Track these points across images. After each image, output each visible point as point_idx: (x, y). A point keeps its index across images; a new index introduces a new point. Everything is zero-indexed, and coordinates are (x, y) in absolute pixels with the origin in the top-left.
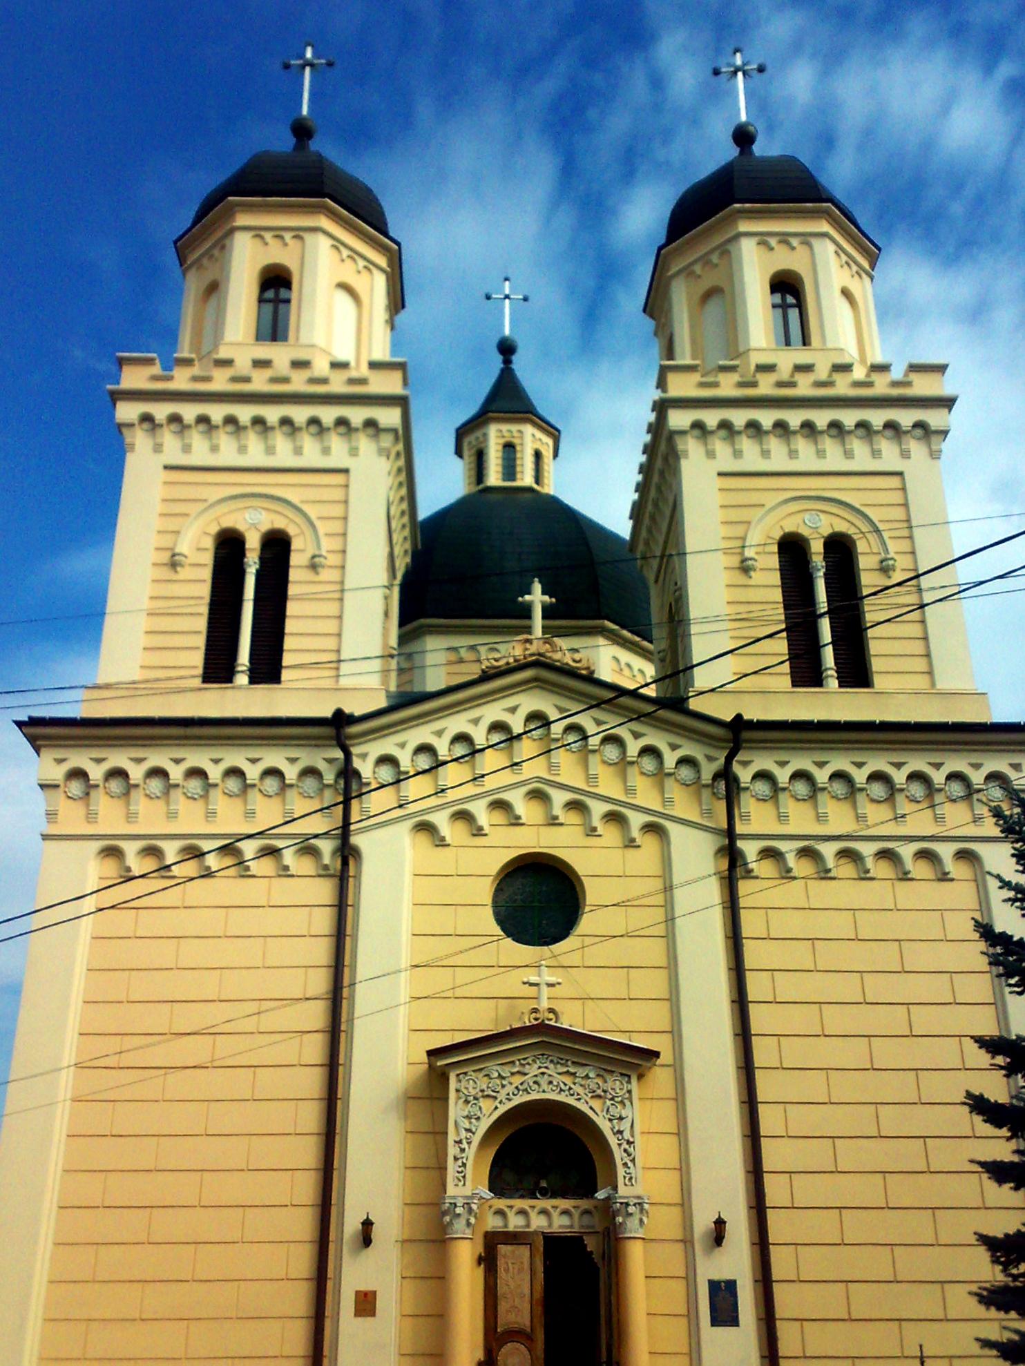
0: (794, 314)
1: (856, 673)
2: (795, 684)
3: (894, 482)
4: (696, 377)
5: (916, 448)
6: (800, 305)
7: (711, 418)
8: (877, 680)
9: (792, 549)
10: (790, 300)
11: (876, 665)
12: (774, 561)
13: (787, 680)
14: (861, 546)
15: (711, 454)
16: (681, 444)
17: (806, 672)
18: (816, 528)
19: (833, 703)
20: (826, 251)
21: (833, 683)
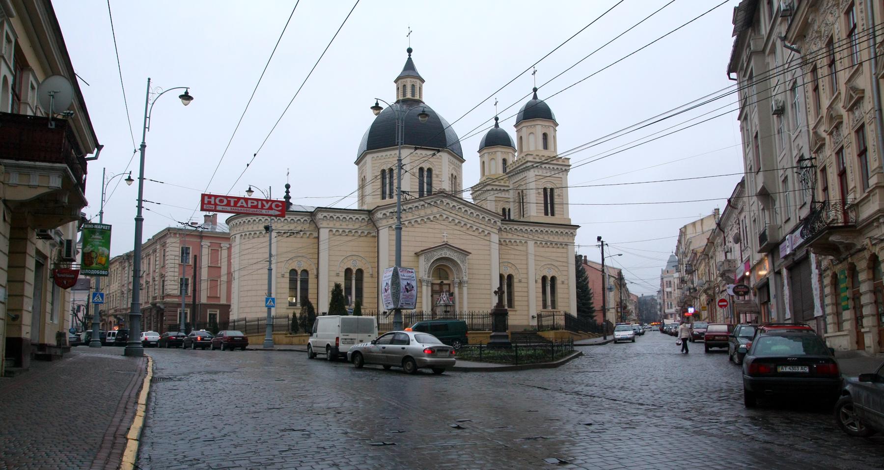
1: (553, 214)
9: (545, 189)
17: (546, 214)
19: (549, 219)
20: (551, 129)
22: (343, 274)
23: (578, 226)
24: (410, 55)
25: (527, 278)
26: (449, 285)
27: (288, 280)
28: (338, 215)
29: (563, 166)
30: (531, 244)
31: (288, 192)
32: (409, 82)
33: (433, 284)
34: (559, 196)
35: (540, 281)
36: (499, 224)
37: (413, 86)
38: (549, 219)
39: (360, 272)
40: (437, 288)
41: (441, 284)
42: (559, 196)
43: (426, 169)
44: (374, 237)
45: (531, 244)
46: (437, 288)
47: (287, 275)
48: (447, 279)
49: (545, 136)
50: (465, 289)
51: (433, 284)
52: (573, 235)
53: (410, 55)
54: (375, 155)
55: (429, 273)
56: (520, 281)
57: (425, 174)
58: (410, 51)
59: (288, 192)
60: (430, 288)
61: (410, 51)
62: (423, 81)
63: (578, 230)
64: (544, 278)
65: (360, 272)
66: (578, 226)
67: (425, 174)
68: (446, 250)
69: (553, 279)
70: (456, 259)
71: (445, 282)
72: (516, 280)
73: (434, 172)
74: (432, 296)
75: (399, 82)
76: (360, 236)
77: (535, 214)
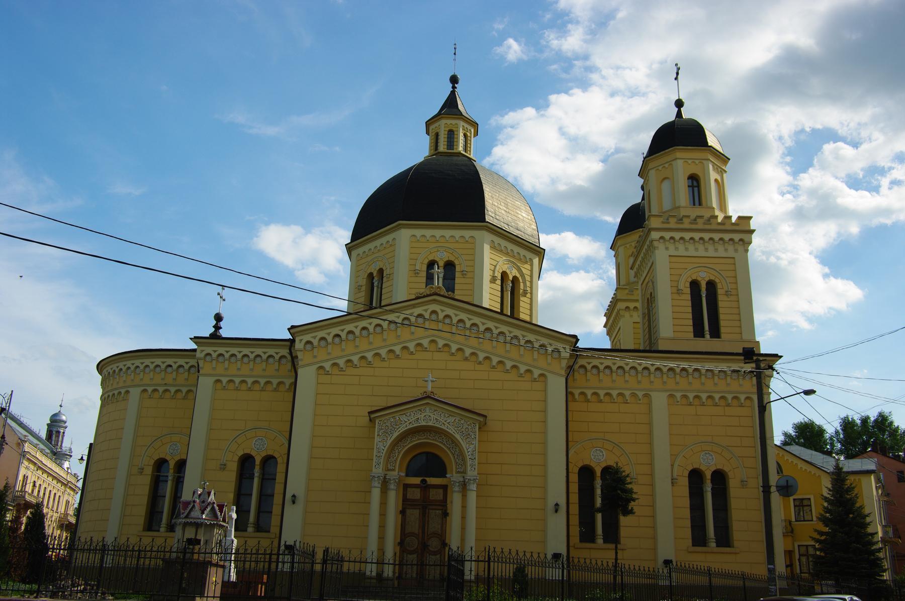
0: (696, 189)
1: (716, 333)
2: (695, 336)
3: (731, 261)
4: (661, 219)
5: (741, 248)
6: (698, 186)
7: (667, 235)
8: (723, 335)
9: (695, 285)
10: (695, 184)
11: (722, 330)
12: (688, 291)
13: (692, 335)
14: (719, 286)
15: (667, 248)
16: (655, 244)
17: (698, 332)
18: (703, 278)
21: (708, 336)
22: (233, 467)
23: (777, 357)
24: (454, 87)
25: (652, 475)
26: (445, 488)
28: (234, 350)
30: (660, 400)
31: (217, 327)
33: (406, 486)
34: (727, 293)
35: (685, 481)
37: (451, 135)
38: (707, 343)
40: (415, 494)
42: (727, 293)
45: (660, 400)
49: (695, 182)
50: (472, 496)
53: (454, 87)
58: (454, 80)
59: (217, 327)
61: (454, 80)
64: (695, 476)
68: (428, 412)
70: (451, 430)
71: (432, 481)
73: (458, 268)
74: (403, 512)
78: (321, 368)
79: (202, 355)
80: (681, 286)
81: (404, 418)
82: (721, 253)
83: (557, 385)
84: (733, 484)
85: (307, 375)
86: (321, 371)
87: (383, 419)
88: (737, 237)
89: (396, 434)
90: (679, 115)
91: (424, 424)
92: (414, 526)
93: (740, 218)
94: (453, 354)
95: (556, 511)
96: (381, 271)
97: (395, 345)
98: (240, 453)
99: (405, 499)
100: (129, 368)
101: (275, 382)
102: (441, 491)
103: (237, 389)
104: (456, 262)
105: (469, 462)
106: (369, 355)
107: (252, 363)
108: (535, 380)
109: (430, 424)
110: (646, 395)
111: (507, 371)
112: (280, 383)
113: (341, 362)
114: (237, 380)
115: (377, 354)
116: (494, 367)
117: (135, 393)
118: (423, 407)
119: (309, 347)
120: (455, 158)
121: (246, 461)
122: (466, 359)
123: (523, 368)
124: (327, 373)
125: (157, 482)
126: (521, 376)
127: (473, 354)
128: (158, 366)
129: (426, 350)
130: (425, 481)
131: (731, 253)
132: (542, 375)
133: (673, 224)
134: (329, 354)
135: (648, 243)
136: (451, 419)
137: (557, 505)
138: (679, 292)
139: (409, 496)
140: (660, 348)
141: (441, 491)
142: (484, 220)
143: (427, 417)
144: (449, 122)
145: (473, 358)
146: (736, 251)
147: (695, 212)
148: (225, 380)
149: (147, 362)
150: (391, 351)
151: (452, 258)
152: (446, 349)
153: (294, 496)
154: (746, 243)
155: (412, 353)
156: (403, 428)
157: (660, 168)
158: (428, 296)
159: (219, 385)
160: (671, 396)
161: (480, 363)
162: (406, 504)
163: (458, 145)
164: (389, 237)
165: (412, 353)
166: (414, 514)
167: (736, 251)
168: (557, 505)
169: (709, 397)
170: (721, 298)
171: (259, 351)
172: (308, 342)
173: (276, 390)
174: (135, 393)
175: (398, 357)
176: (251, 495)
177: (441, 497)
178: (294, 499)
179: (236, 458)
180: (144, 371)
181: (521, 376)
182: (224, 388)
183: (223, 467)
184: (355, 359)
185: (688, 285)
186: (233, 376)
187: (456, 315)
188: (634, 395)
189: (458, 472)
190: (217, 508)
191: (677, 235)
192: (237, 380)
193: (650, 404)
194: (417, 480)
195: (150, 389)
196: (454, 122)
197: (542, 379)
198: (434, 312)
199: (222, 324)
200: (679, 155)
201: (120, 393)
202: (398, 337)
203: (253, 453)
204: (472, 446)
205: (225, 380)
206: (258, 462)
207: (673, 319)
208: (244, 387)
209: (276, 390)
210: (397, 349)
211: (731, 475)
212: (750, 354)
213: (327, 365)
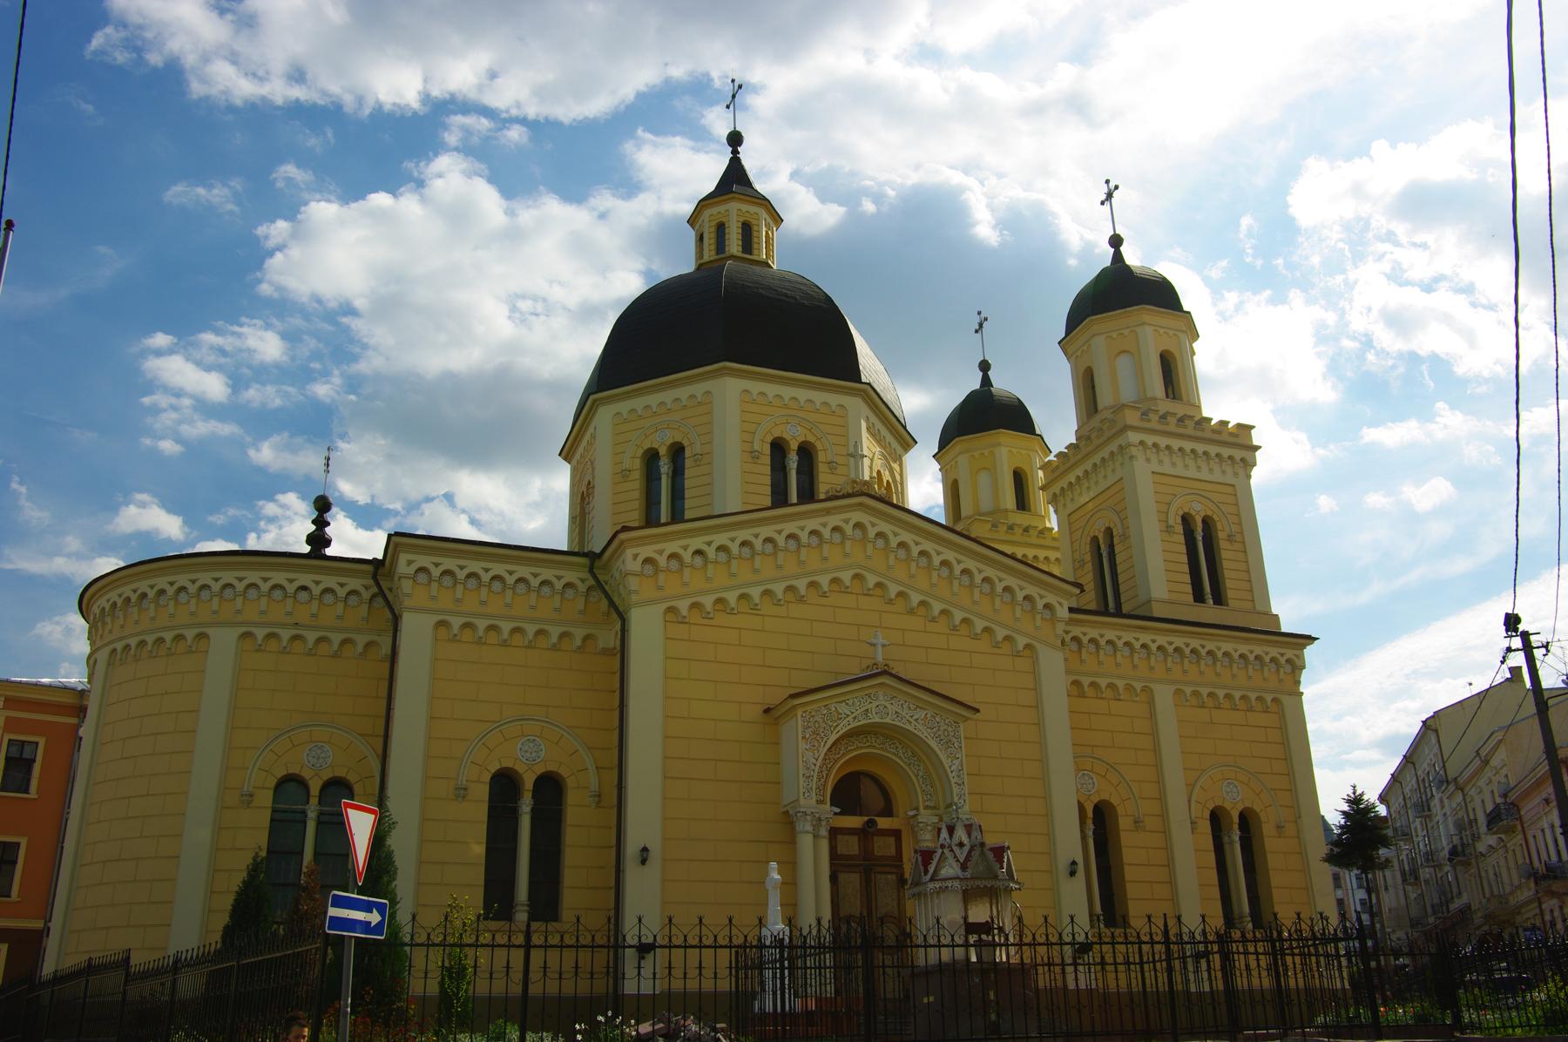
1: (1219, 599)
3: (1230, 490)
5: (1241, 472)
7: (1150, 439)
9: (1186, 520)
11: (1230, 594)
12: (1180, 529)
15: (1148, 460)
17: (1199, 597)
18: (1198, 510)
22: (482, 792)
23: (1311, 639)
24: (735, 152)
26: (896, 834)
27: (265, 819)
29: (1237, 445)
30: (1164, 696)
32: (734, 211)
34: (1230, 538)
35: (1205, 827)
36: (1063, 613)
38: (1208, 612)
39: (550, 787)
40: (850, 846)
41: (867, 833)
42: (1230, 538)
43: (794, 446)
44: (606, 652)
46: (850, 846)
47: (266, 799)
48: (888, 812)
51: (834, 832)
52: (1296, 667)
53: (735, 152)
54: (624, 407)
55: (821, 789)
56: (1137, 823)
57: (793, 462)
60: (824, 845)
62: (778, 220)
63: (1309, 652)
64: (1217, 819)
65: (550, 787)
66: (1311, 639)
67: (793, 462)
69: (1247, 821)
70: (923, 733)
71: (883, 823)
72: (1124, 823)
73: (821, 457)
74: (834, 878)
75: (707, 213)
76: (555, 648)
77: (1166, 596)
78: (671, 610)
79: (412, 569)
80: (1171, 522)
81: (843, 709)
82: (1217, 476)
83: (1053, 664)
84: (1268, 830)
85: (416, 629)
86: (670, 617)
87: (809, 708)
88: (1238, 454)
89: (833, 738)
90: (1118, 257)
91: (877, 719)
92: (853, 906)
93: (1239, 426)
94: (890, 602)
95: (1072, 873)
96: (677, 451)
97: (797, 577)
98: (494, 768)
99: (834, 855)
100: (162, 592)
101: (555, 631)
102: (891, 840)
103: (480, 642)
104: (819, 447)
105: (955, 790)
106: (755, 592)
107: (315, 603)
108: (1017, 655)
109: (888, 720)
110: (1144, 689)
111: (976, 637)
112: (564, 635)
113: (708, 601)
114: (482, 624)
115: (767, 593)
116: (954, 628)
117: (224, 641)
118: (872, 691)
119: (649, 569)
120: (757, 269)
121: (504, 785)
122: (911, 612)
123: (1001, 633)
124: (683, 621)
125: (284, 823)
126: (997, 645)
127: (923, 603)
128: (205, 587)
129: (846, 591)
130: (871, 823)
131: (1229, 479)
132: (1027, 646)
133: (1154, 424)
134: (660, 588)
135: (1113, 447)
136: (921, 714)
137: (1074, 863)
138: (1168, 529)
139: (841, 850)
140: (1156, 615)
141: (891, 840)
142: (859, 380)
143: (882, 707)
144: (745, 207)
145: (922, 611)
146: (1236, 474)
147: (1166, 406)
148: (456, 622)
149: (253, 576)
150: (790, 588)
151: (811, 439)
152: (878, 592)
153: (645, 849)
154: (1248, 464)
155: (824, 595)
156: (843, 728)
157: (1114, 335)
158: (849, 496)
159: (442, 631)
160: (1178, 692)
161: (933, 620)
162: (838, 864)
163: (760, 249)
164: (698, 389)
165: (824, 595)
166: (851, 881)
167: (1236, 474)
168: (1074, 863)
169: (1227, 696)
170: (1223, 544)
171: (523, 571)
172: (647, 561)
173: (581, 649)
174: (224, 641)
175: (801, 600)
176: (15, 862)
177: (893, 852)
178: (644, 855)
179: (487, 777)
180: (198, 595)
181: (997, 645)
182: (454, 639)
183: (461, 793)
184: (732, 597)
185: (1179, 520)
186: (475, 615)
187: (896, 535)
188: (1129, 687)
189: (927, 807)
190: (990, 855)
191: (1163, 442)
192: (482, 624)
193: (1151, 702)
194: (855, 822)
195: (260, 633)
196: (753, 209)
197: (1027, 653)
198: (858, 525)
199: (328, 516)
200: (1147, 318)
201: (143, 643)
202: (801, 563)
203: (520, 768)
204: (957, 762)
205: (456, 622)
206: (315, 789)
207: (1159, 570)
208: (517, 640)
209: (555, 648)
210: (801, 585)
211: (1263, 816)
212: (1270, 631)
213: (683, 606)
